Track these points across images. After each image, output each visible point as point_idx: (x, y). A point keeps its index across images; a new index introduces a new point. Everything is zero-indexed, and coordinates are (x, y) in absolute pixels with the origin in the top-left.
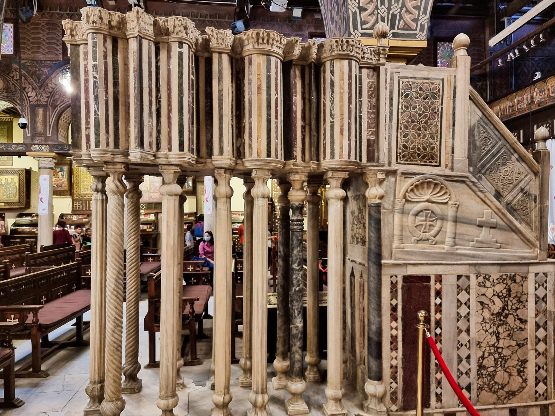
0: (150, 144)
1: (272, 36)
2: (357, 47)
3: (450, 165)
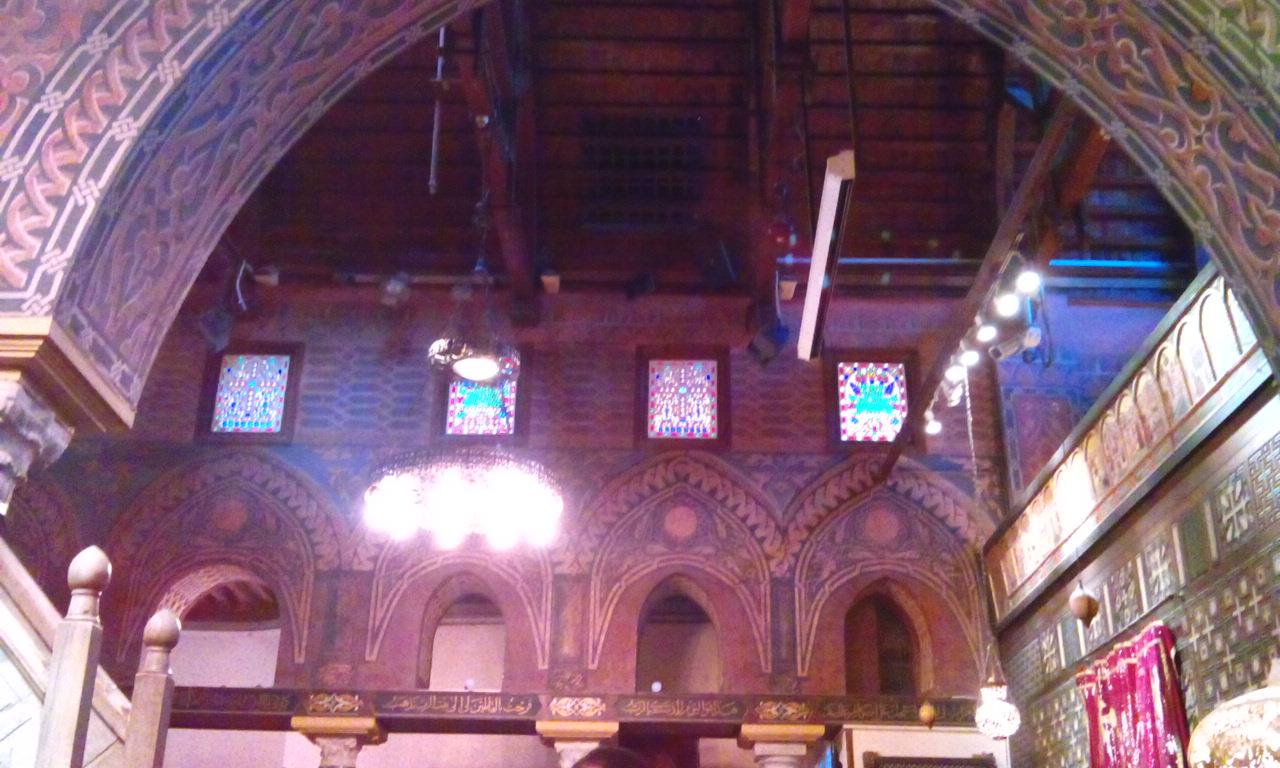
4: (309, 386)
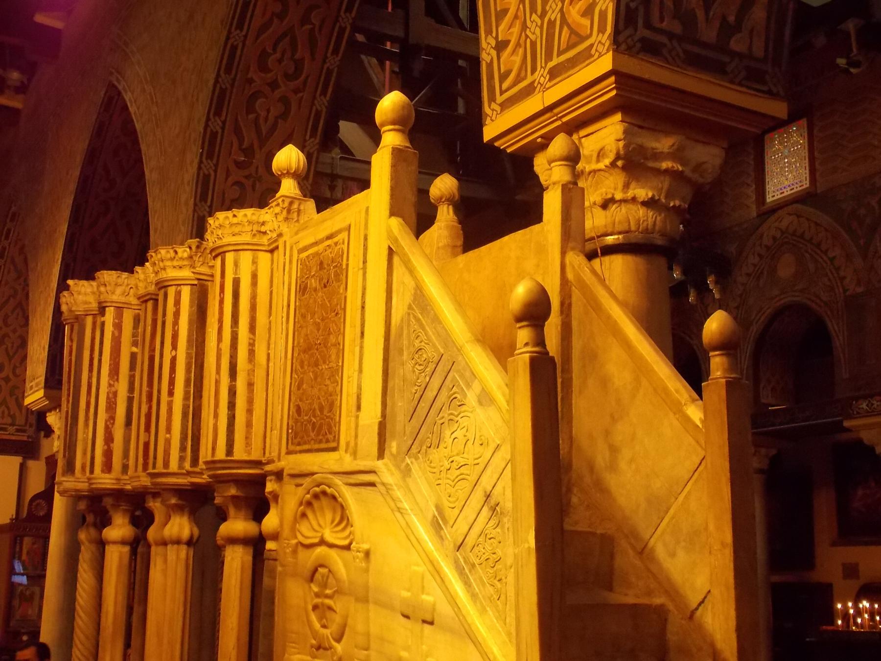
2: (231, 225)
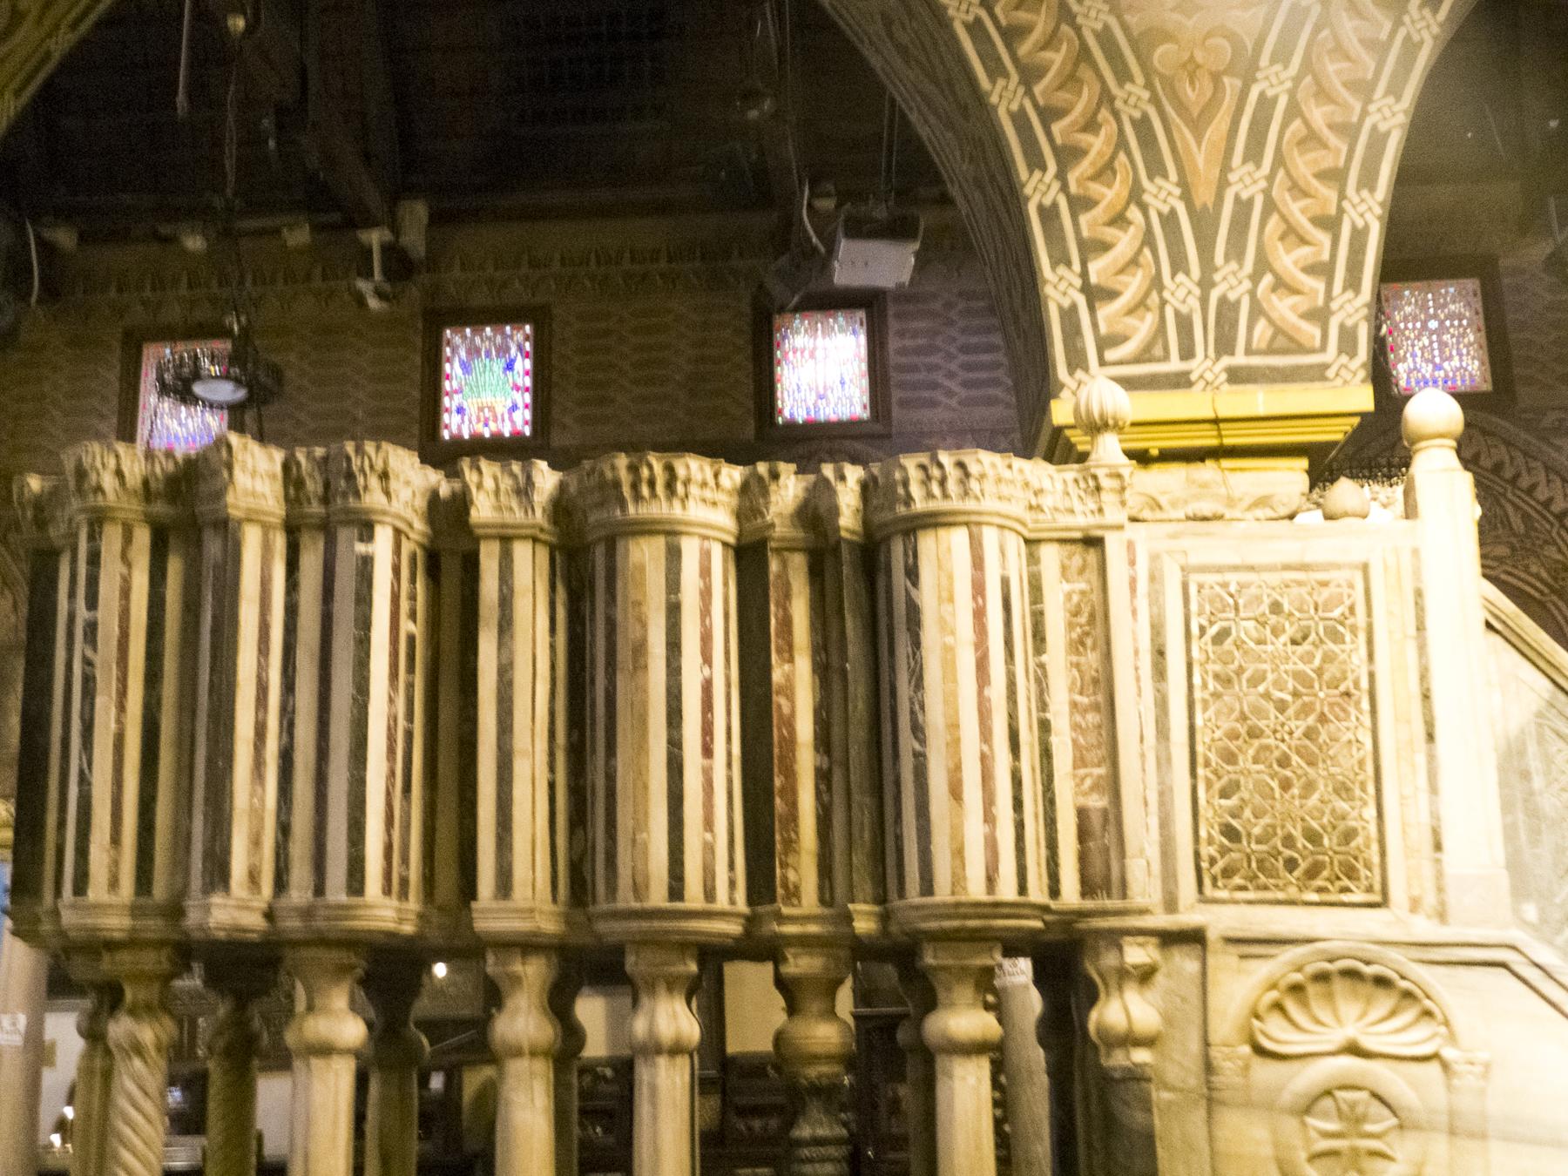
0: (253, 878)
1: (681, 472)
2: (999, 480)
3: (1430, 899)
4: (903, 352)
